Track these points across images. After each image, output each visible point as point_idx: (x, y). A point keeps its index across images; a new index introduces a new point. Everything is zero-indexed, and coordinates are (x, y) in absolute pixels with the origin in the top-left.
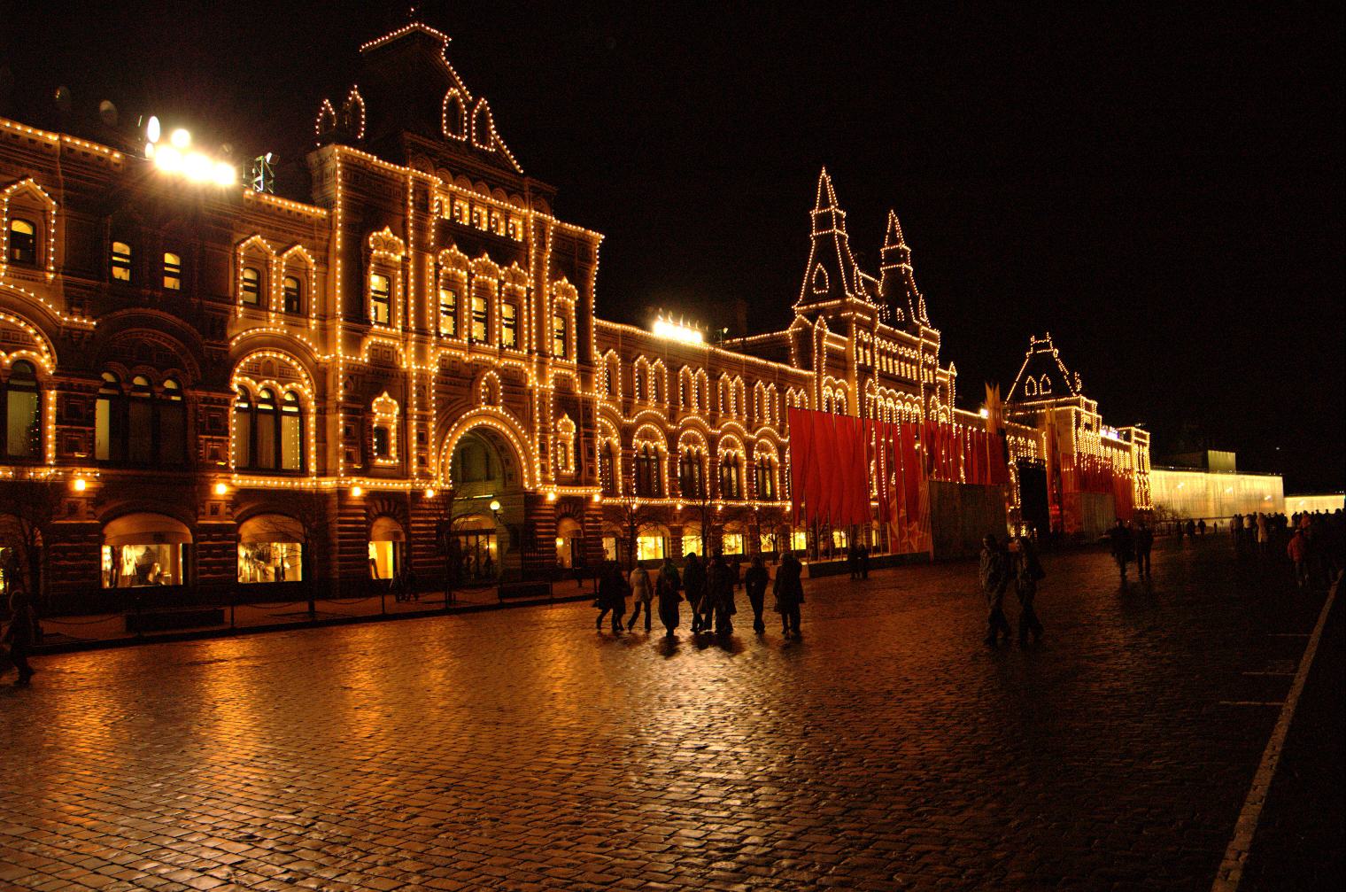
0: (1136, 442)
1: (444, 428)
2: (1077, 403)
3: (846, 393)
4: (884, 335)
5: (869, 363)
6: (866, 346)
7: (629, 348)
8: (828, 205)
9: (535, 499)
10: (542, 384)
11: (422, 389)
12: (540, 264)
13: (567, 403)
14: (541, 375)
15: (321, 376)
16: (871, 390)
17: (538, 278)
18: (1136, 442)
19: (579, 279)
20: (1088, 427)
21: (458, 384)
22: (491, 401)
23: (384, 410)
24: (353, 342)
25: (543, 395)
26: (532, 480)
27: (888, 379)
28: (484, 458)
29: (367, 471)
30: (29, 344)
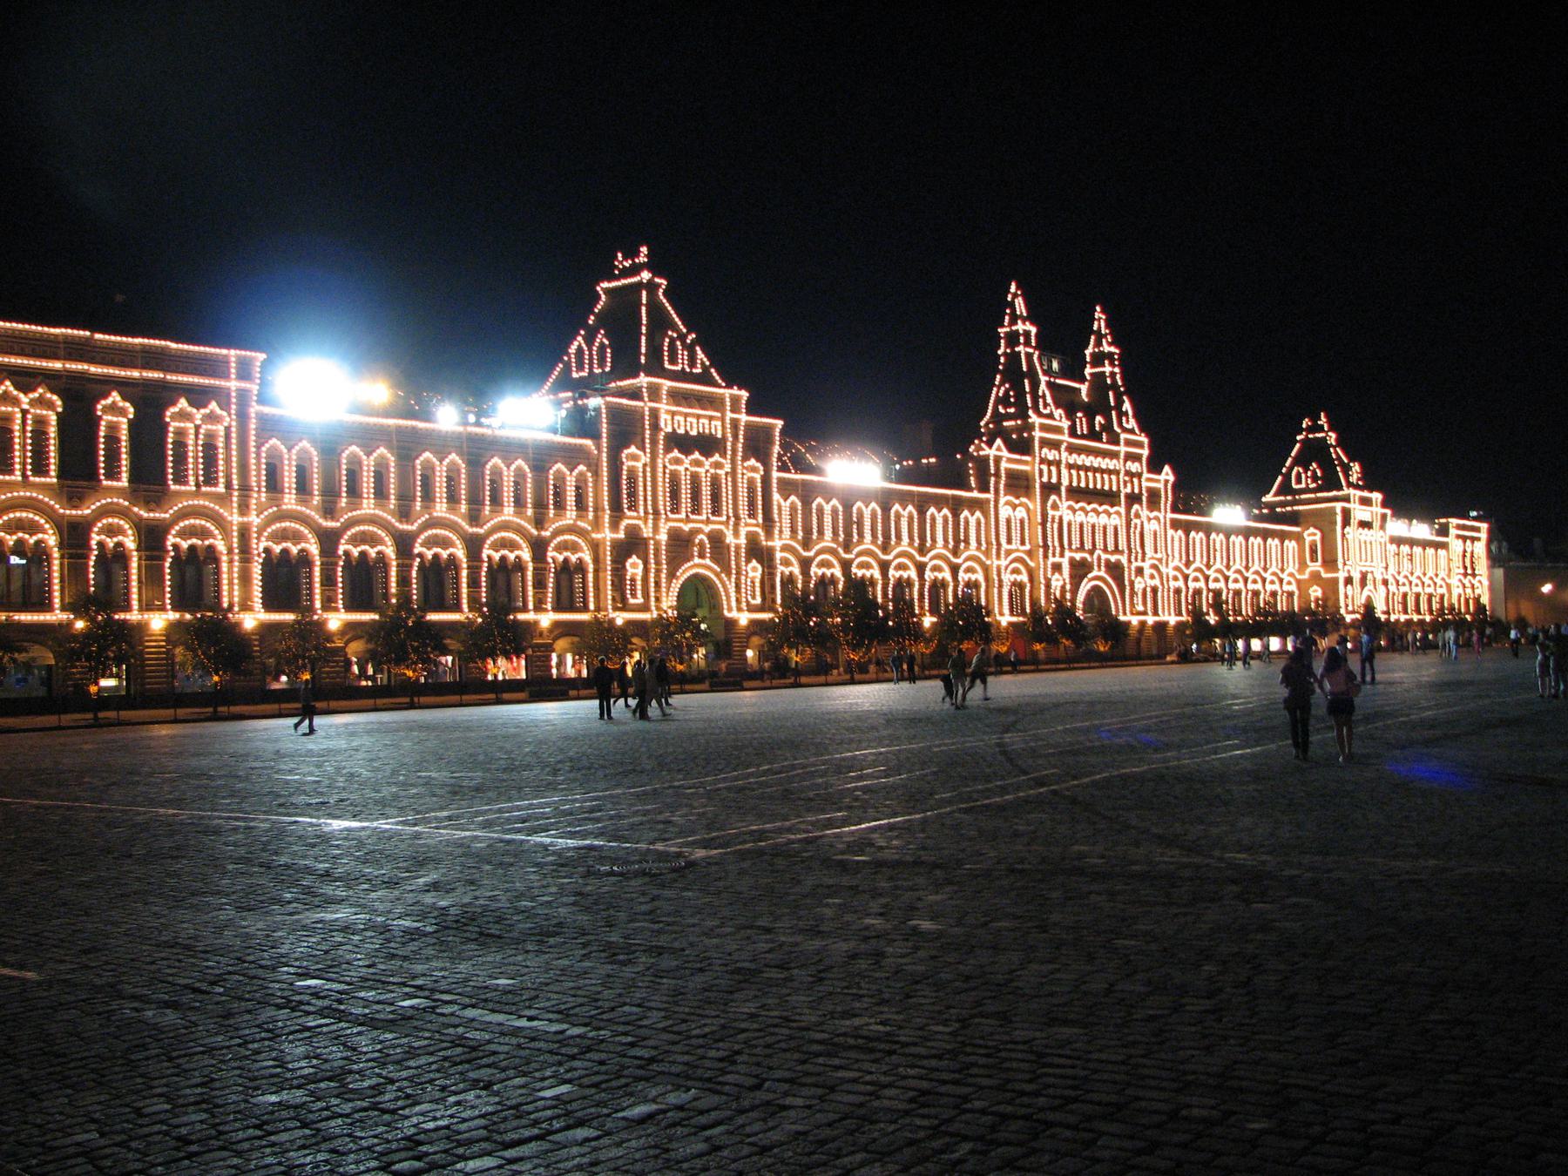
0: (1458, 537)
1: (672, 575)
2: (1347, 499)
3: (1028, 510)
4: (1072, 449)
5: (1054, 480)
6: (1050, 463)
7: (807, 493)
8: (1020, 324)
9: (731, 624)
10: (736, 540)
11: (657, 551)
12: (734, 451)
13: (757, 551)
14: (736, 534)
15: (595, 547)
16: (1055, 507)
17: (733, 462)
18: (1458, 537)
19: (764, 459)
20: (1365, 525)
21: (681, 545)
22: (702, 556)
23: (634, 566)
24: (615, 526)
25: (738, 547)
26: (730, 610)
27: (1076, 493)
28: (698, 593)
29: (625, 607)
30: (452, 545)
